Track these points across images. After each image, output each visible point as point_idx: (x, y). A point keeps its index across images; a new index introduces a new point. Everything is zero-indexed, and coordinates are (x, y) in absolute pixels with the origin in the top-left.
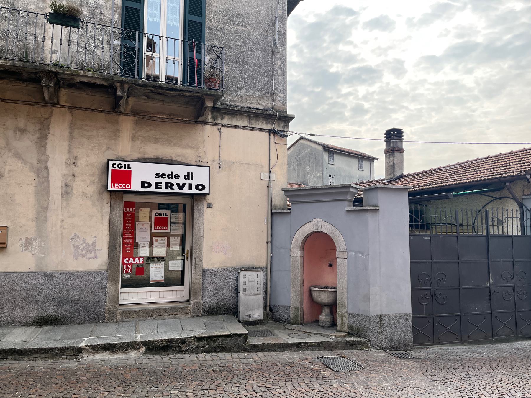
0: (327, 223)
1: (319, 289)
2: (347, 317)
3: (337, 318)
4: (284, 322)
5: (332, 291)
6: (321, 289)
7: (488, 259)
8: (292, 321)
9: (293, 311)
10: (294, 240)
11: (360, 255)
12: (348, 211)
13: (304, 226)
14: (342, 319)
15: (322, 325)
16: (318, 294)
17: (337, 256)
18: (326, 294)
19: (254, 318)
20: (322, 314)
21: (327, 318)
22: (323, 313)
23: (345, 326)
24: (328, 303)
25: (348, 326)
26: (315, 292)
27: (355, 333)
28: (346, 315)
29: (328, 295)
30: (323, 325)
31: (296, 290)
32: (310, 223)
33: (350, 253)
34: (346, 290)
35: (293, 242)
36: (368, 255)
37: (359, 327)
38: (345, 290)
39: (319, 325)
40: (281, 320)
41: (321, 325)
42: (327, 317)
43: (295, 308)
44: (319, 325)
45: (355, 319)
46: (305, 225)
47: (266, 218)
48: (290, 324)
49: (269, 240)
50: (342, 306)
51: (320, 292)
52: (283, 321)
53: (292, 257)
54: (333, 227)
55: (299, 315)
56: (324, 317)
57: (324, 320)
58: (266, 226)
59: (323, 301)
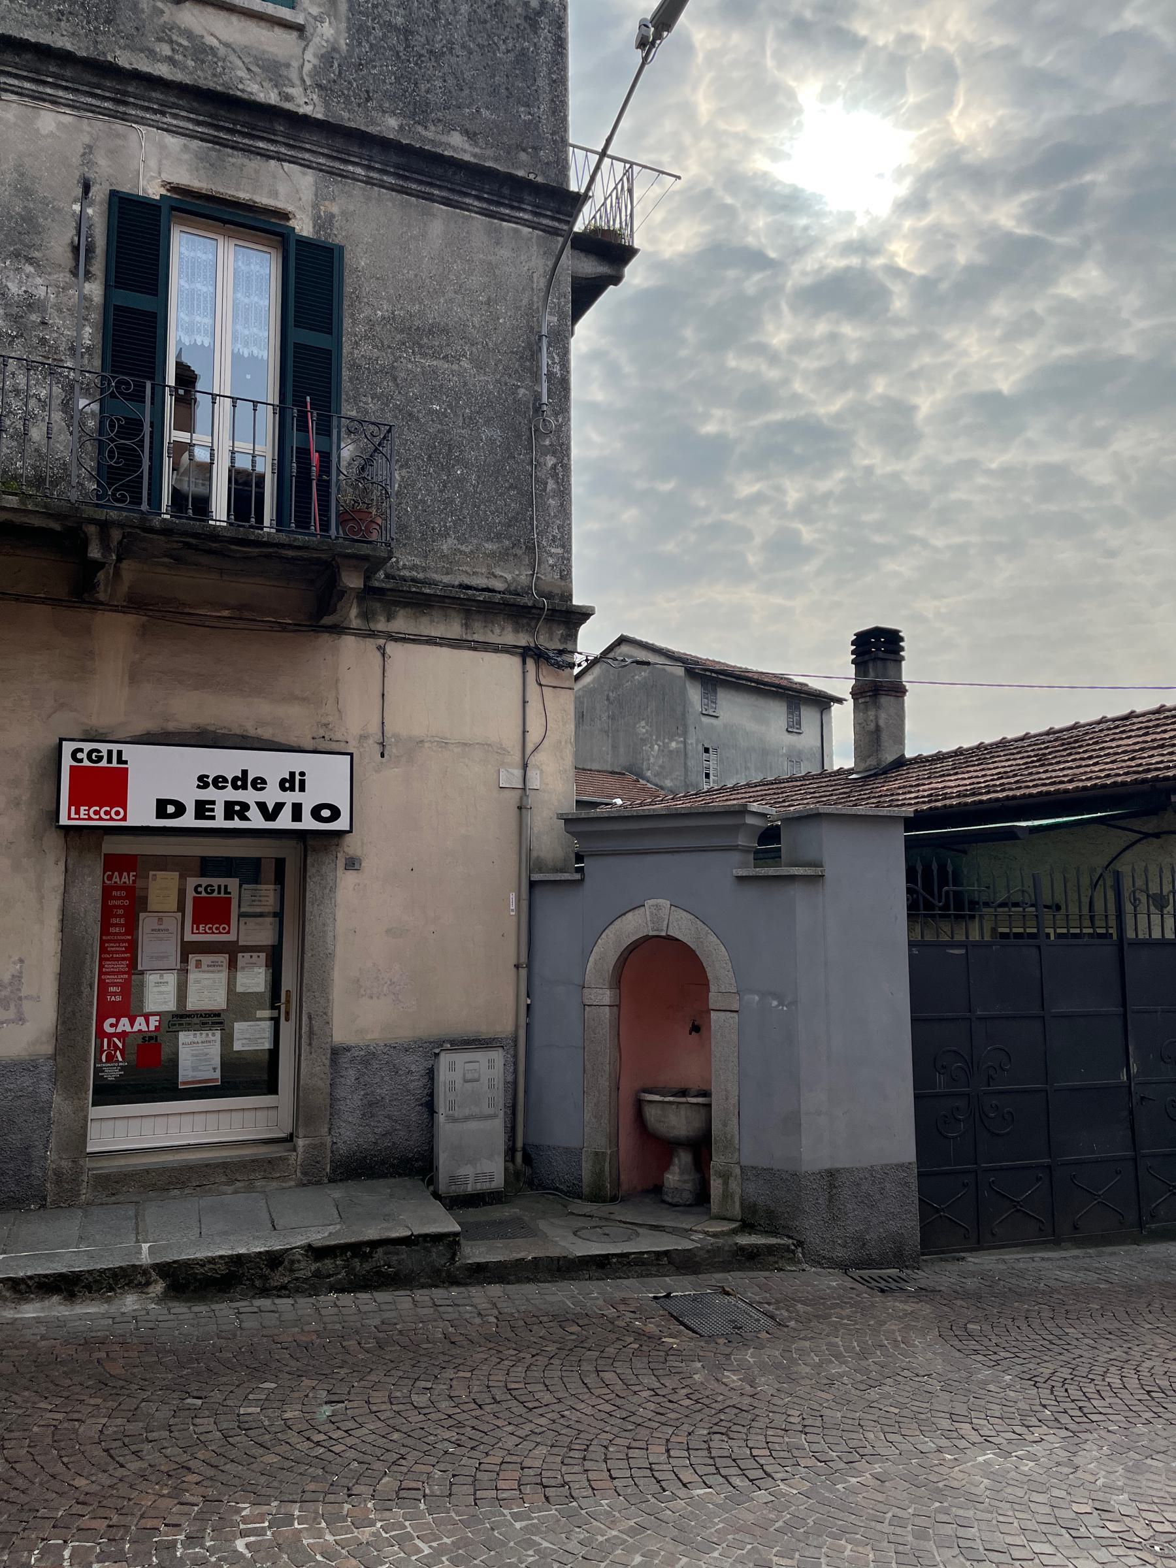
0: (685, 913)
3: (712, 1182)
5: (697, 1104)
6: (667, 1099)
7: (1124, 1004)
8: (586, 1190)
10: (592, 959)
11: (775, 1003)
12: (740, 879)
14: (726, 1183)
16: (659, 1112)
19: (479, 1186)
20: (672, 1168)
21: (685, 1182)
23: (734, 1202)
25: (741, 1204)
27: (762, 1223)
28: (737, 1171)
32: (636, 912)
35: (590, 964)
36: (795, 1002)
38: (734, 1101)
39: (664, 1202)
40: (557, 1189)
41: (669, 1199)
42: (686, 1177)
43: (596, 1154)
44: (664, 1202)
46: (624, 917)
47: (513, 896)
48: (580, 1198)
49: (524, 959)
50: (726, 1147)
52: (561, 1191)
53: (586, 1007)
54: (699, 922)
55: (607, 1173)
56: (677, 1178)
58: (515, 919)
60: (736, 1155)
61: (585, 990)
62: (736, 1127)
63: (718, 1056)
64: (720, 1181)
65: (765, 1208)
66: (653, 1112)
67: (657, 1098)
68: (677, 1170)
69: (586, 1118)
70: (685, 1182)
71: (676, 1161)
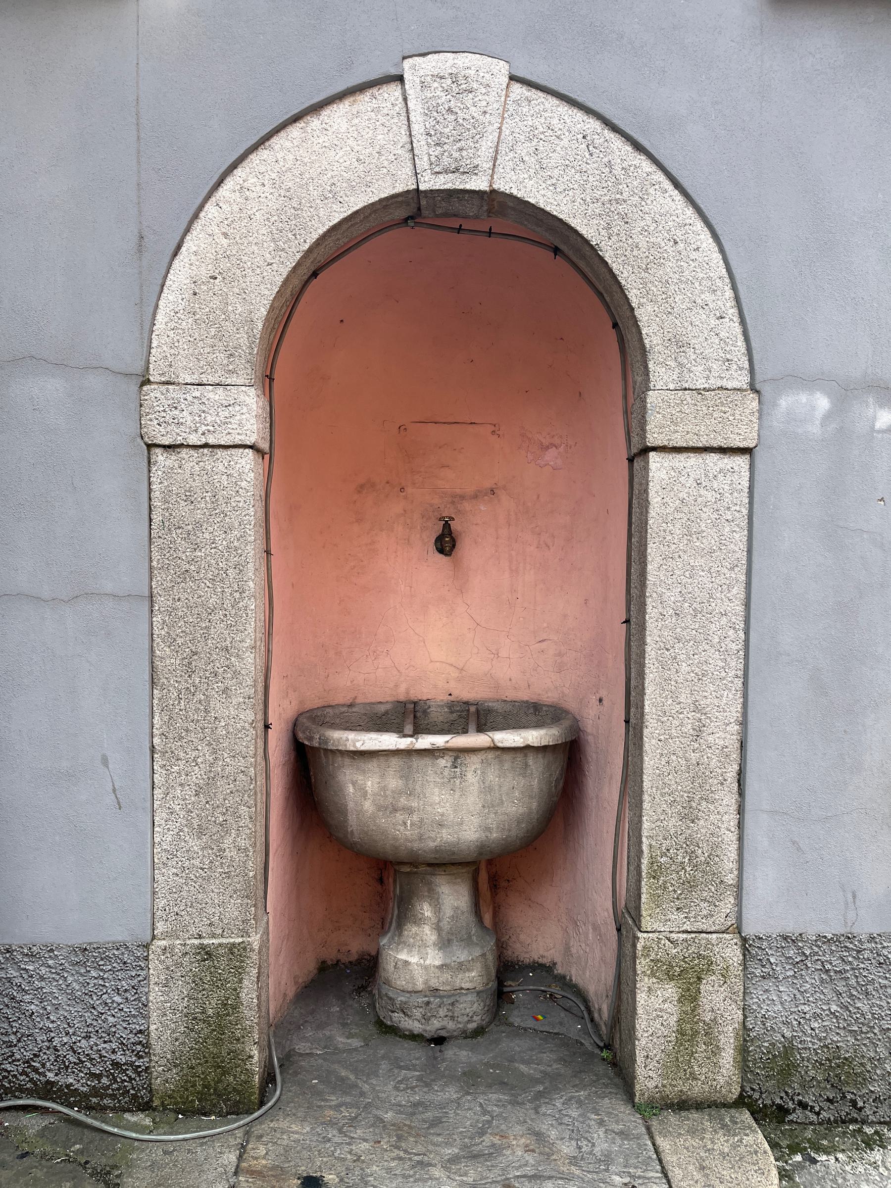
0: (564, 109)
1: (404, 743)
2: (736, 969)
3: (641, 997)
4: (83, 1102)
5: (527, 749)
9: (180, 989)
13: (295, 131)
15: (414, 1025)
16: (394, 783)
17: (654, 438)
18: (471, 778)
20: (411, 930)
21: (461, 967)
22: (419, 921)
23: (717, 1051)
24: (482, 848)
25: (743, 1051)
26: (373, 765)
27: (809, 1099)
28: (732, 954)
29: (492, 777)
30: (434, 1026)
31: (211, 781)
32: (364, 101)
33: (785, 402)
34: (732, 742)
35: (170, 299)
37: (846, 1043)
40: (48, 1090)
42: (462, 955)
43: (206, 954)
45: (811, 980)
46: (314, 123)
48: (146, 1107)
50: (691, 885)
51: (417, 762)
52: (66, 1095)
53: (160, 456)
54: (617, 143)
55: (250, 1015)
56: (434, 958)
57: (434, 983)
59: (446, 836)
60: (728, 904)
61: (153, 393)
62: (731, 819)
63: (672, 596)
64: (671, 991)
65: (823, 1055)
66: (371, 784)
67: (389, 741)
68: (428, 933)
69: (164, 837)
70: (461, 967)
71: (426, 910)
